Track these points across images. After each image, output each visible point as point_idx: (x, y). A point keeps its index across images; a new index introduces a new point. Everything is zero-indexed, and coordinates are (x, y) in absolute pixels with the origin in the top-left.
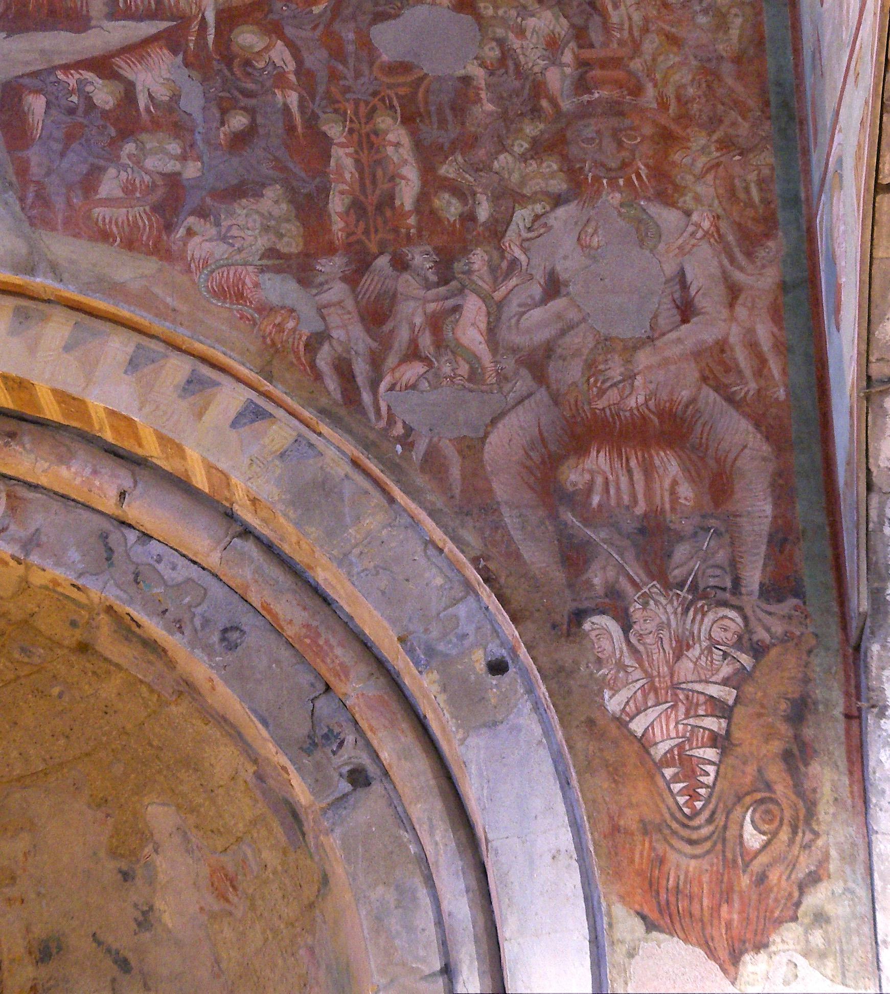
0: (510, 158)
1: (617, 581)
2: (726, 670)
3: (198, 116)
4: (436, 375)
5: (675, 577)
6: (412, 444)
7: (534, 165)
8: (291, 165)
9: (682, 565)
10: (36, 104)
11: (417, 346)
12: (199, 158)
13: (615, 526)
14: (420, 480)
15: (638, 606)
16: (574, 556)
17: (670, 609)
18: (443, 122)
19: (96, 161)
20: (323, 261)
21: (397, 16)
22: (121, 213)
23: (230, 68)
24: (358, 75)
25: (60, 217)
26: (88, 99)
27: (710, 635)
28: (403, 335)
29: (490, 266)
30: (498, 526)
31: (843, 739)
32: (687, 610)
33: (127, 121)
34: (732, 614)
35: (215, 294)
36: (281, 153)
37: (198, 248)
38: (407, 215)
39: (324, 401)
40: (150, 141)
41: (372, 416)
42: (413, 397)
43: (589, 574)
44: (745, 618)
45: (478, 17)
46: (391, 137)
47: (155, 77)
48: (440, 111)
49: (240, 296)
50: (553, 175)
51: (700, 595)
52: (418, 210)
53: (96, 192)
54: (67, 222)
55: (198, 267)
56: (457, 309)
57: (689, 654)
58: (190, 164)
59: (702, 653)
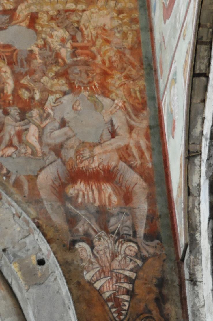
0: (47, 79)
1: (88, 230)
2: (132, 266)
5: (111, 230)
6: (9, 177)
7: (56, 81)
9: (113, 225)
13: (87, 209)
14: (13, 190)
15: (97, 240)
16: (72, 220)
17: (109, 241)
27: (125, 252)
30: (43, 208)
31: (179, 295)
32: (115, 243)
34: (133, 245)
42: (10, 160)
43: (77, 227)
44: (138, 247)
50: (63, 85)
51: (120, 237)
57: (117, 259)
59: (122, 259)
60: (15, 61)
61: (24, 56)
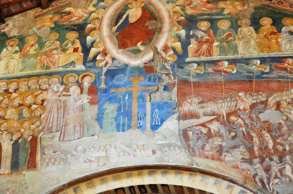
3: (224, 133)
4: (282, 181)
8: (245, 142)
10: (190, 133)
11: (277, 176)
12: (226, 141)
18: (276, 132)
19: (204, 143)
20: (255, 160)
21: (263, 112)
22: (210, 153)
23: (230, 124)
24: (257, 124)
25: (198, 155)
26: (201, 131)
28: (274, 174)
29: (290, 159)
33: (209, 135)
35: (232, 168)
36: (243, 140)
37: (227, 159)
38: (271, 150)
39: (258, 188)
40: (215, 139)
41: (269, 190)
42: (278, 186)
45: (281, 111)
46: (266, 135)
47: (215, 127)
48: (275, 129)
49: (238, 168)
52: (273, 149)
53: (205, 149)
54: (199, 155)
55: (228, 162)
56: (284, 168)
58: (224, 142)
60: (271, 130)
61: (276, 127)
